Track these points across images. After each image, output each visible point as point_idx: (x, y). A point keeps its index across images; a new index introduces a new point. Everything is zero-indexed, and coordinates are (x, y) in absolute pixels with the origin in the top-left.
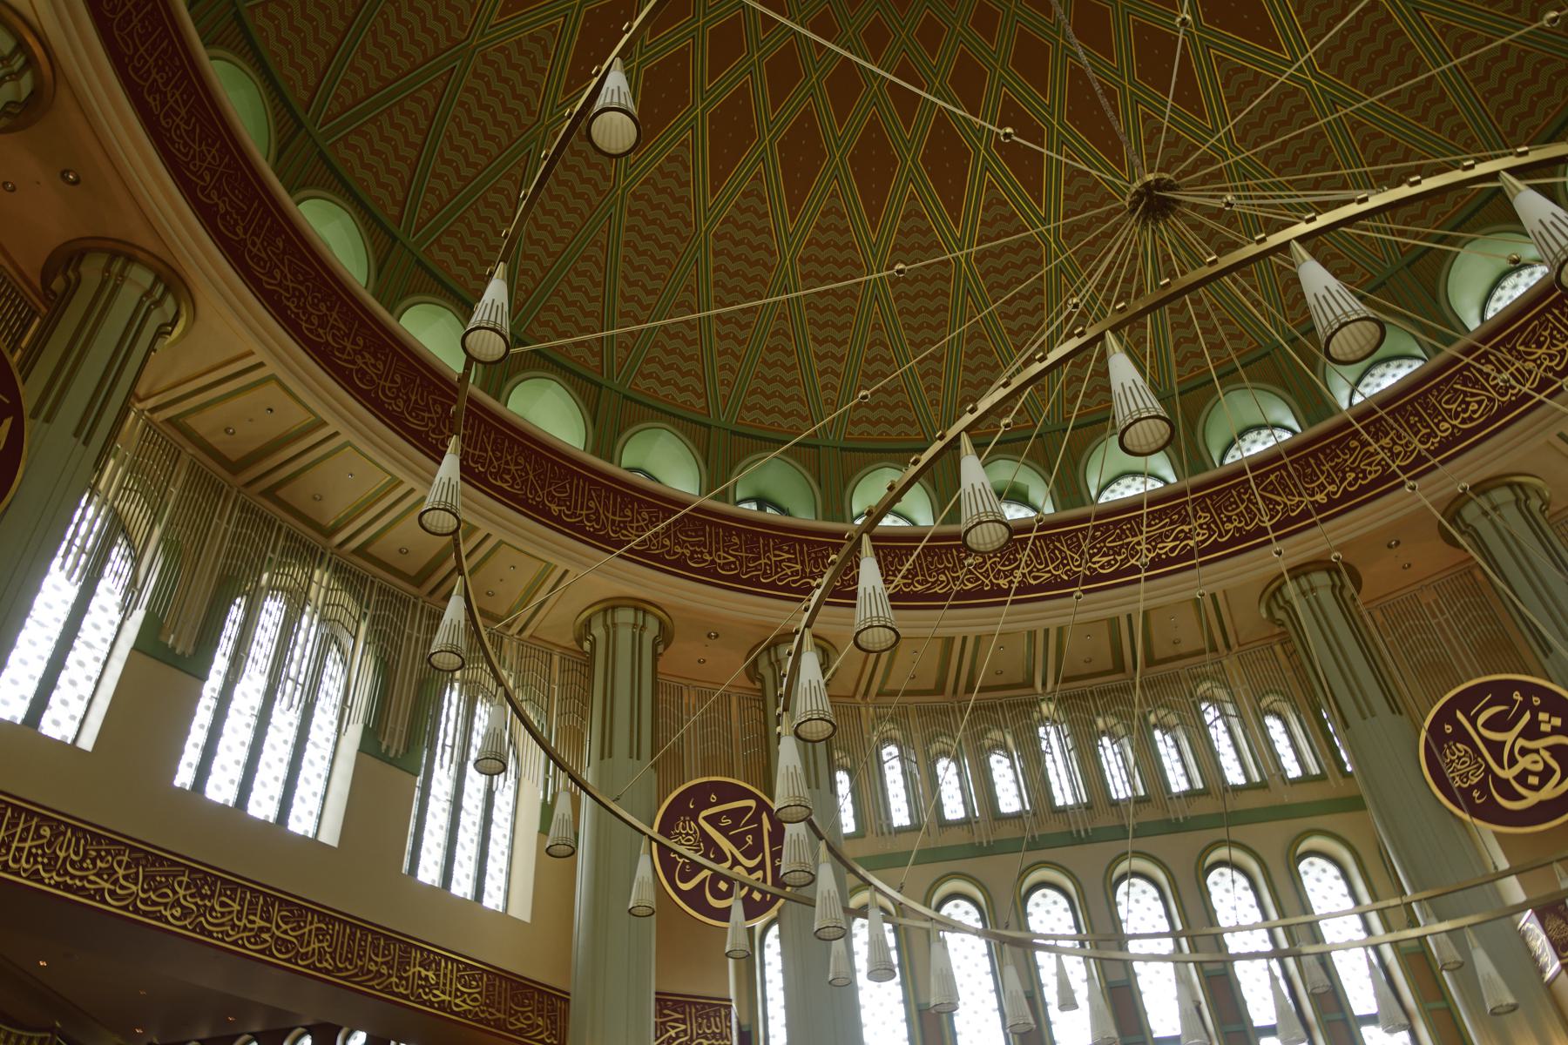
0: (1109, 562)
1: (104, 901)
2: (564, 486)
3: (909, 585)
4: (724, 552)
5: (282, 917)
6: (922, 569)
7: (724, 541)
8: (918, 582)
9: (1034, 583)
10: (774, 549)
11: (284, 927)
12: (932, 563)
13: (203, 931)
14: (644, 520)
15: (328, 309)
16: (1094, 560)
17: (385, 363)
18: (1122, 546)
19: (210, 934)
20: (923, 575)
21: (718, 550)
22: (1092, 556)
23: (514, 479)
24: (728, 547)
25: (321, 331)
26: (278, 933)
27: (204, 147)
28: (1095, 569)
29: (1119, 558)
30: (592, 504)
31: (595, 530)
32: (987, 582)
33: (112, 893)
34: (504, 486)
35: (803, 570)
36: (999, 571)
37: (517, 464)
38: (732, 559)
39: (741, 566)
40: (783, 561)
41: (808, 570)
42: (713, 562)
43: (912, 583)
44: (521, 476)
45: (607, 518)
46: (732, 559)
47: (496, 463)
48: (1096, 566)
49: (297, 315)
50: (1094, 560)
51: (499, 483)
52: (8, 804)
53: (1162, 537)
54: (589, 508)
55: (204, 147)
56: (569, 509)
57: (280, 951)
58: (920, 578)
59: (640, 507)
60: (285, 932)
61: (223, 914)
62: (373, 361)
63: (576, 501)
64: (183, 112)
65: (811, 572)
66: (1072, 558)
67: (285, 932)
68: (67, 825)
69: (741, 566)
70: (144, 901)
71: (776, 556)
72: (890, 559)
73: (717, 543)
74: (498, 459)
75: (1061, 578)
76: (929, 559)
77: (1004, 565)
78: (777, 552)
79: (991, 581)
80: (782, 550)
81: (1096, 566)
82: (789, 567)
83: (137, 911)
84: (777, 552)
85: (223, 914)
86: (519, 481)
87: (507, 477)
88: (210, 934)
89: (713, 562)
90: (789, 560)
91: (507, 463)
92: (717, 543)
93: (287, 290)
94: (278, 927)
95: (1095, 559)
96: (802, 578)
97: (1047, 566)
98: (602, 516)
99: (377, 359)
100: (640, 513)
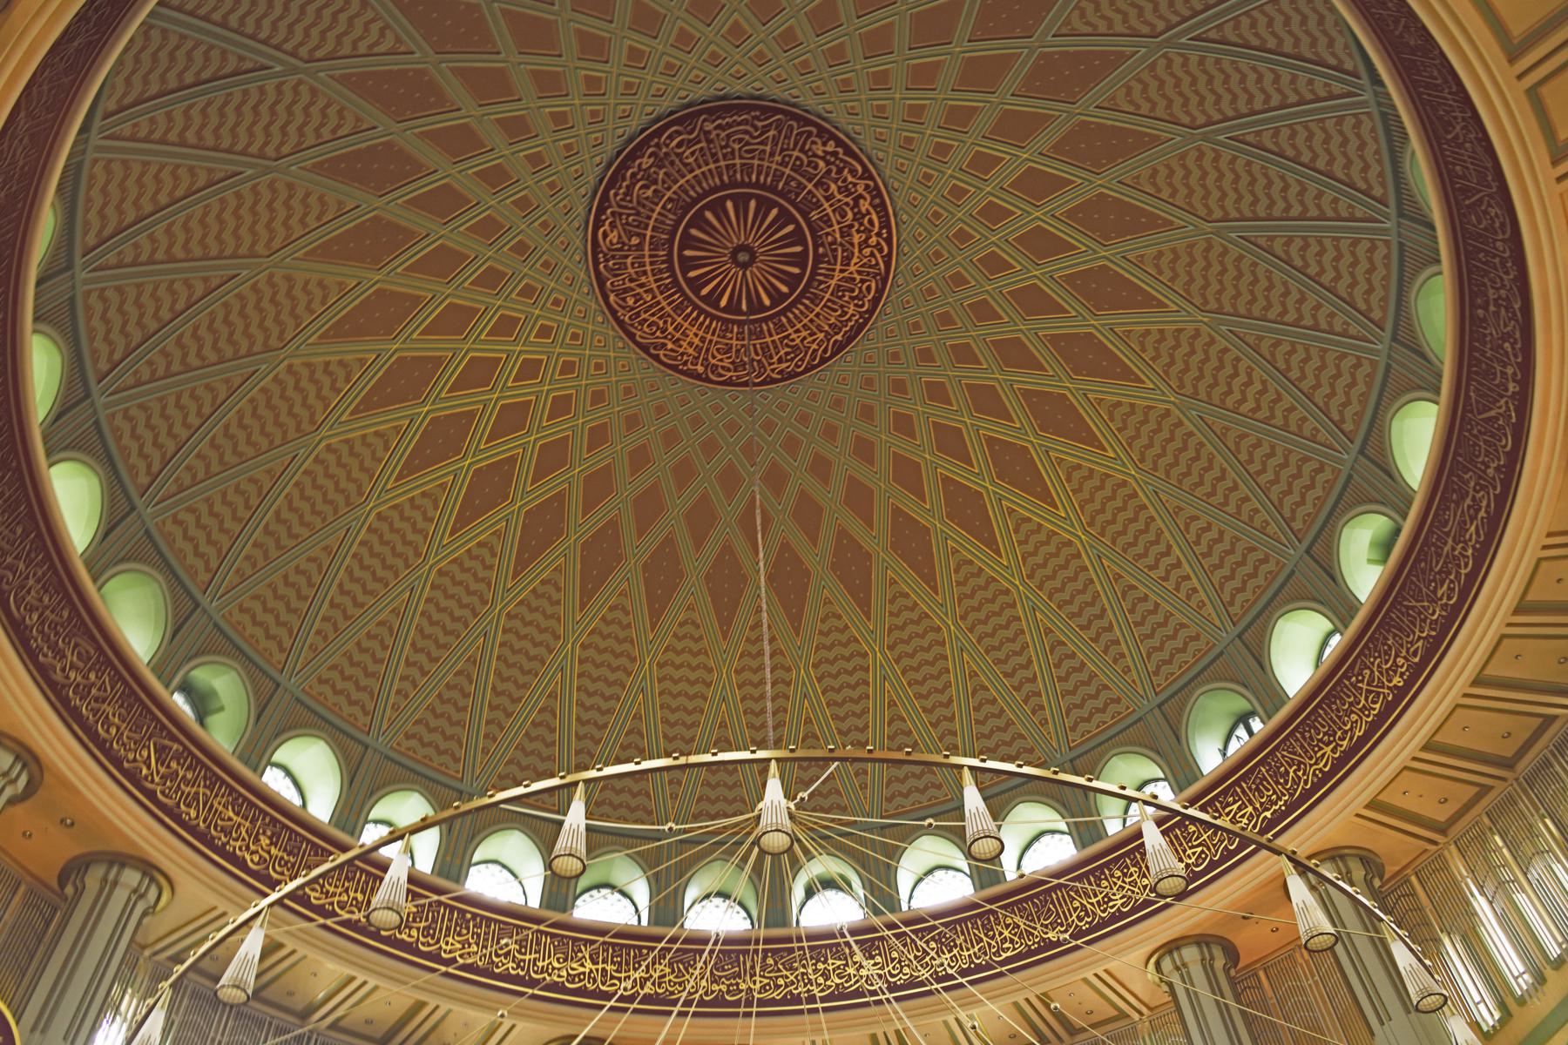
0: (1449, 588)
2: (1049, 909)
3: (1335, 748)
4: (1191, 848)
6: (1334, 722)
7: (1185, 838)
8: (1340, 739)
9: (1417, 660)
10: (1224, 809)
12: (1311, 738)
14: (1119, 878)
15: (824, 963)
16: (1439, 595)
17: (880, 954)
18: (1445, 562)
20: (1340, 729)
21: (1184, 851)
22: (1435, 592)
23: (1012, 941)
24: (1190, 841)
25: (829, 983)
27: (691, 970)
28: (1446, 605)
29: (1452, 577)
30: (1076, 904)
31: (1090, 923)
32: (1386, 691)
34: (1009, 954)
35: (1255, 809)
36: (1387, 670)
37: (1007, 926)
38: (1199, 849)
39: (1209, 849)
40: (1236, 814)
41: (1258, 806)
42: (1187, 866)
43: (1337, 745)
44: (1015, 935)
45: (1092, 904)
46: (1199, 849)
47: (993, 943)
48: (1444, 601)
49: (809, 991)
50: (1439, 595)
51: (1004, 955)
53: (1463, 528)
54: (1075, 909)
55: (691, 970)
56: (1062, 926)
58: (1339, 733)
59: (1110, 870)
62: (872, 962)
63: (1064, 913)
64: (668, 970)
65: (1262, 804)
66: (1423, 607)
69: (1209, 849)
71: (1228, 814)
72: (1307, 735)
73: (1181, 845)
74: (993, 938)
75: (1431, 637)
76: (1334, 707)
77: (1387, 662)
78: (1227, 810)
79: (1389, 688)
80: (1228, 805)
81: (1444, 601)
82: (1243, 816)
84: (1227, 810)
86: (1016, 939)
87: (1005, 946)
89: (1187, 866)
90: (1240, 809)
91: (1001, 934)
92: (1181, 845)
93: (793, 983)
95: (1440, 593)
96: (1258, 817)
97: (1414, 633)
98: (1089, 906)
99: (872, 957)
100: (1112, 876)
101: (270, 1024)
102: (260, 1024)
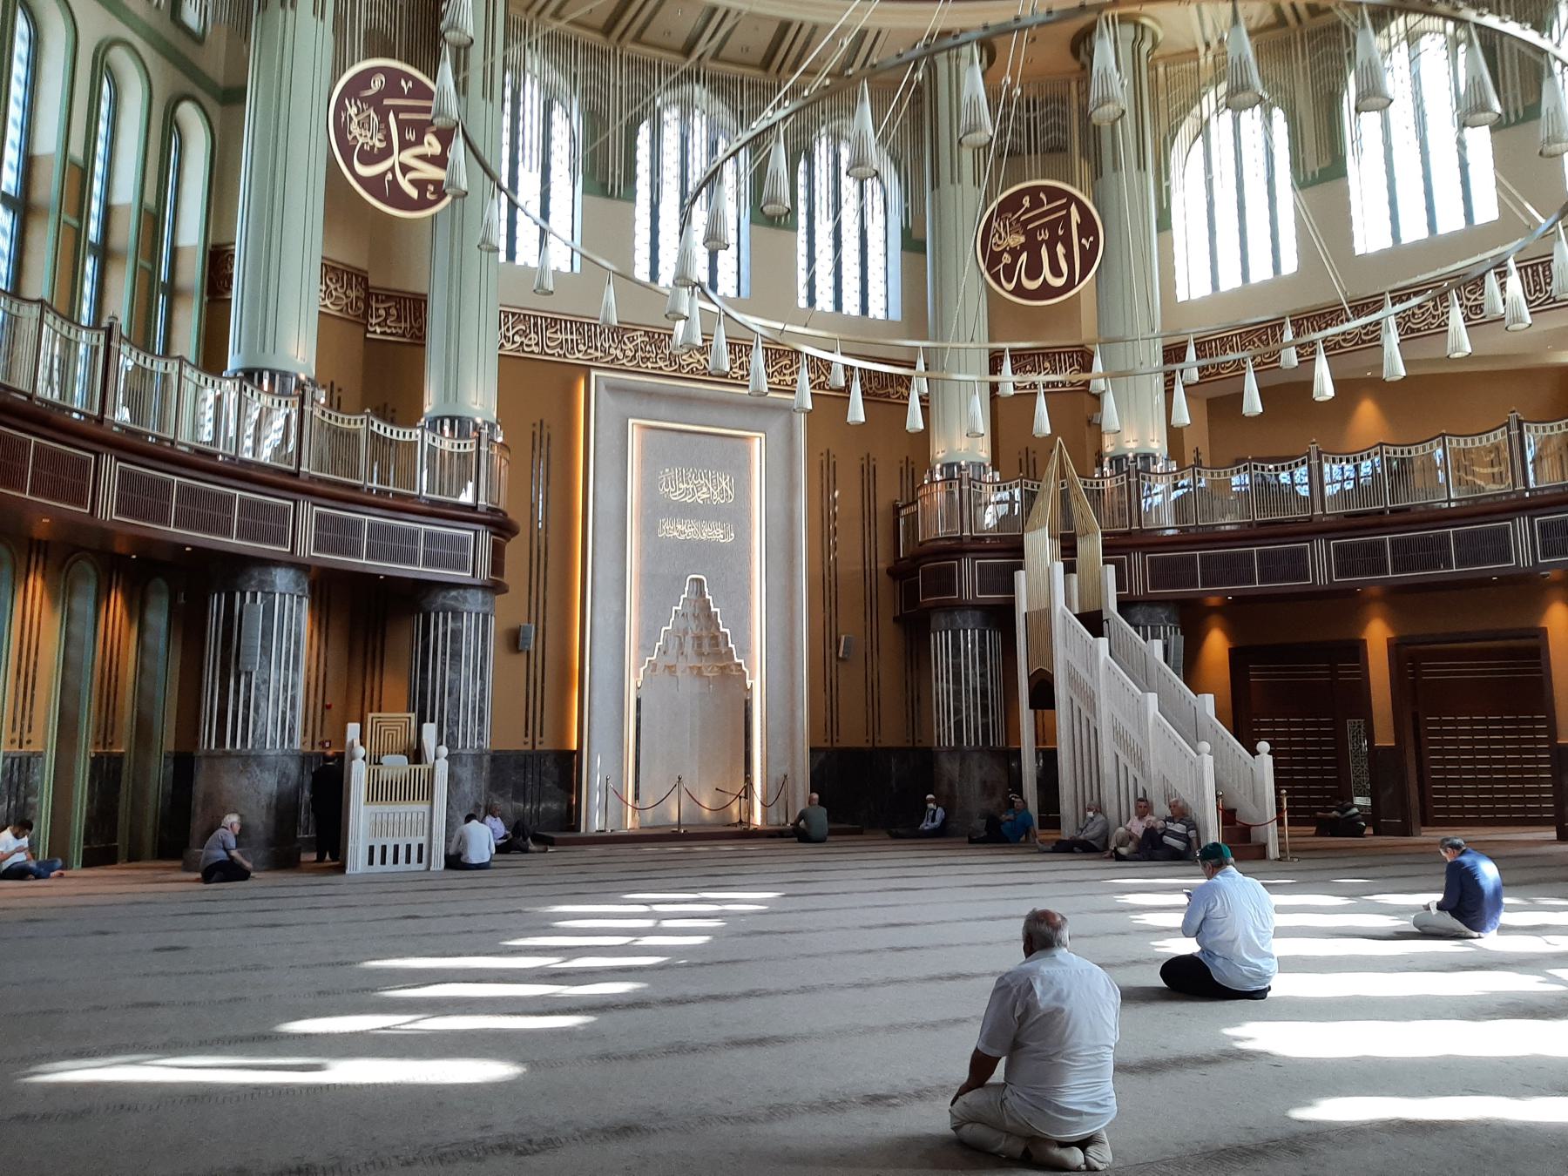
1: (1341, 347)
5: (1469, 292)
11: (1473, 297)
13: (1413, 331)
19: (1419, 330)
26: (1470, 304)
33: (1344, 340)
52: (1267, 327)
57: (1476, 314)
60: (1476, 299)
61: (1423, 314)
67: (1476, 299)
68: (1302, 319)
70: (1366, 334)
83: (1364, 342)
85: (1423, 314)
88: (1419, 330)
94: (1468, 299)
101: (660, 65)
102: (651, 66)
